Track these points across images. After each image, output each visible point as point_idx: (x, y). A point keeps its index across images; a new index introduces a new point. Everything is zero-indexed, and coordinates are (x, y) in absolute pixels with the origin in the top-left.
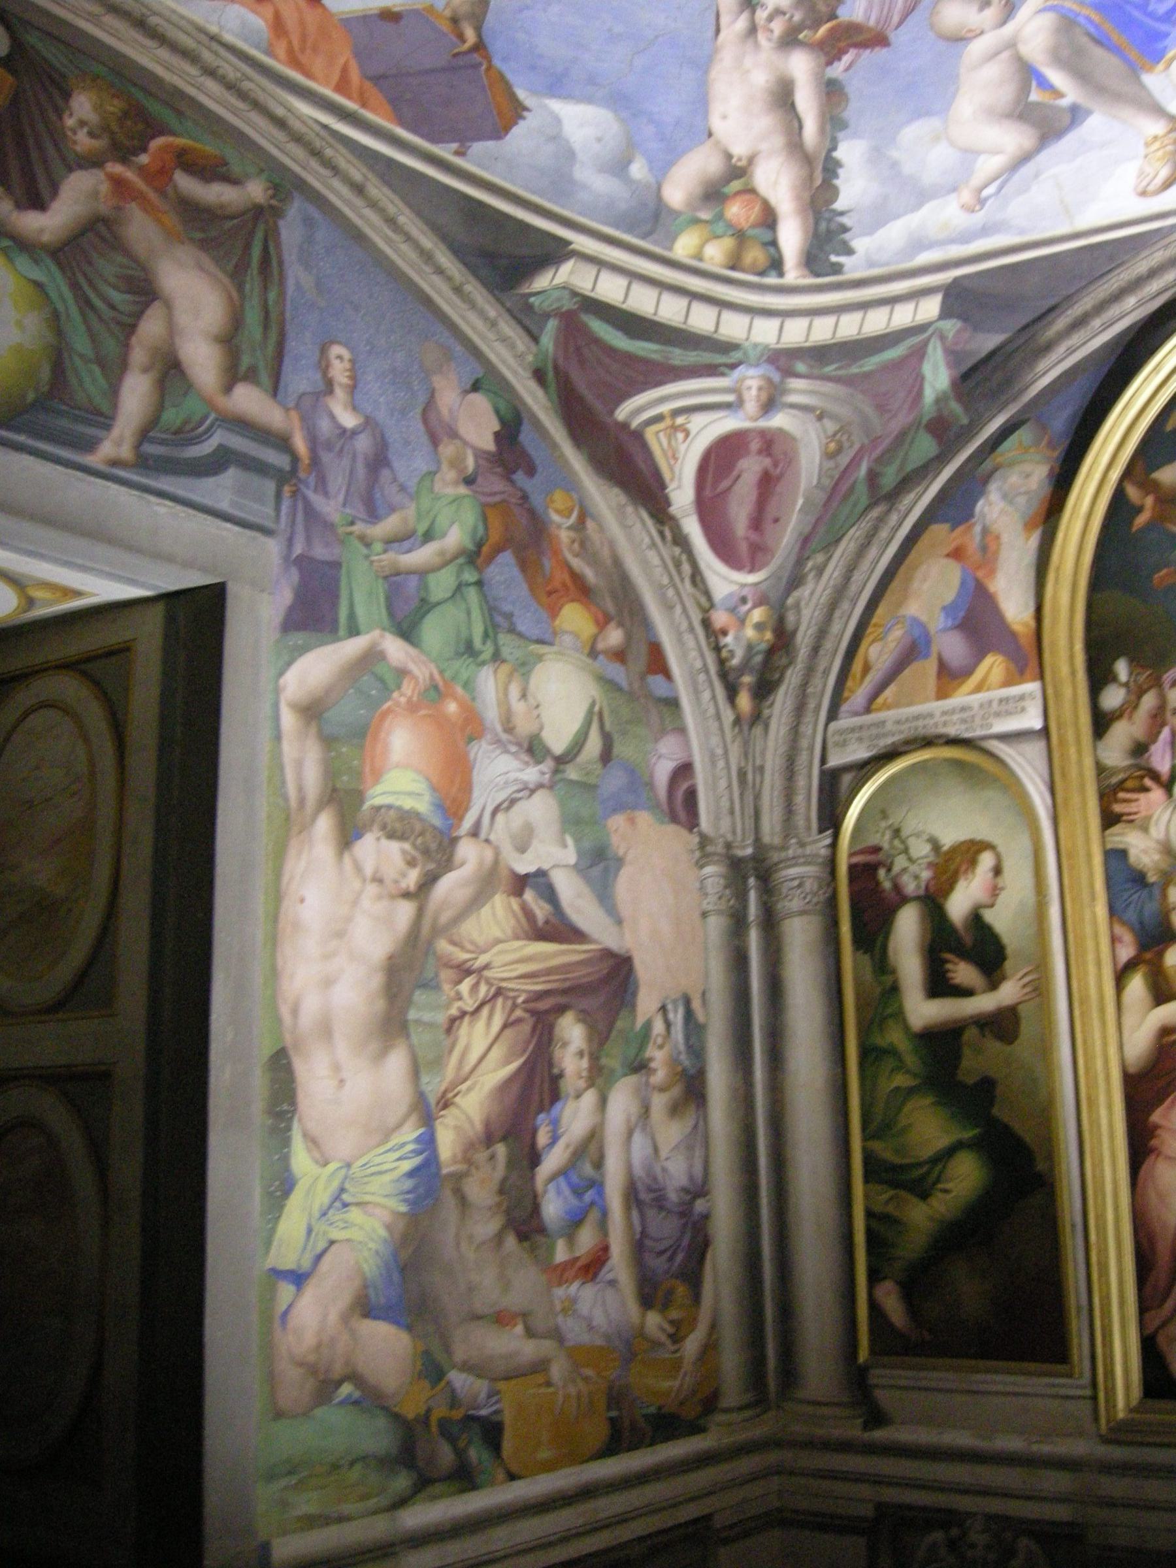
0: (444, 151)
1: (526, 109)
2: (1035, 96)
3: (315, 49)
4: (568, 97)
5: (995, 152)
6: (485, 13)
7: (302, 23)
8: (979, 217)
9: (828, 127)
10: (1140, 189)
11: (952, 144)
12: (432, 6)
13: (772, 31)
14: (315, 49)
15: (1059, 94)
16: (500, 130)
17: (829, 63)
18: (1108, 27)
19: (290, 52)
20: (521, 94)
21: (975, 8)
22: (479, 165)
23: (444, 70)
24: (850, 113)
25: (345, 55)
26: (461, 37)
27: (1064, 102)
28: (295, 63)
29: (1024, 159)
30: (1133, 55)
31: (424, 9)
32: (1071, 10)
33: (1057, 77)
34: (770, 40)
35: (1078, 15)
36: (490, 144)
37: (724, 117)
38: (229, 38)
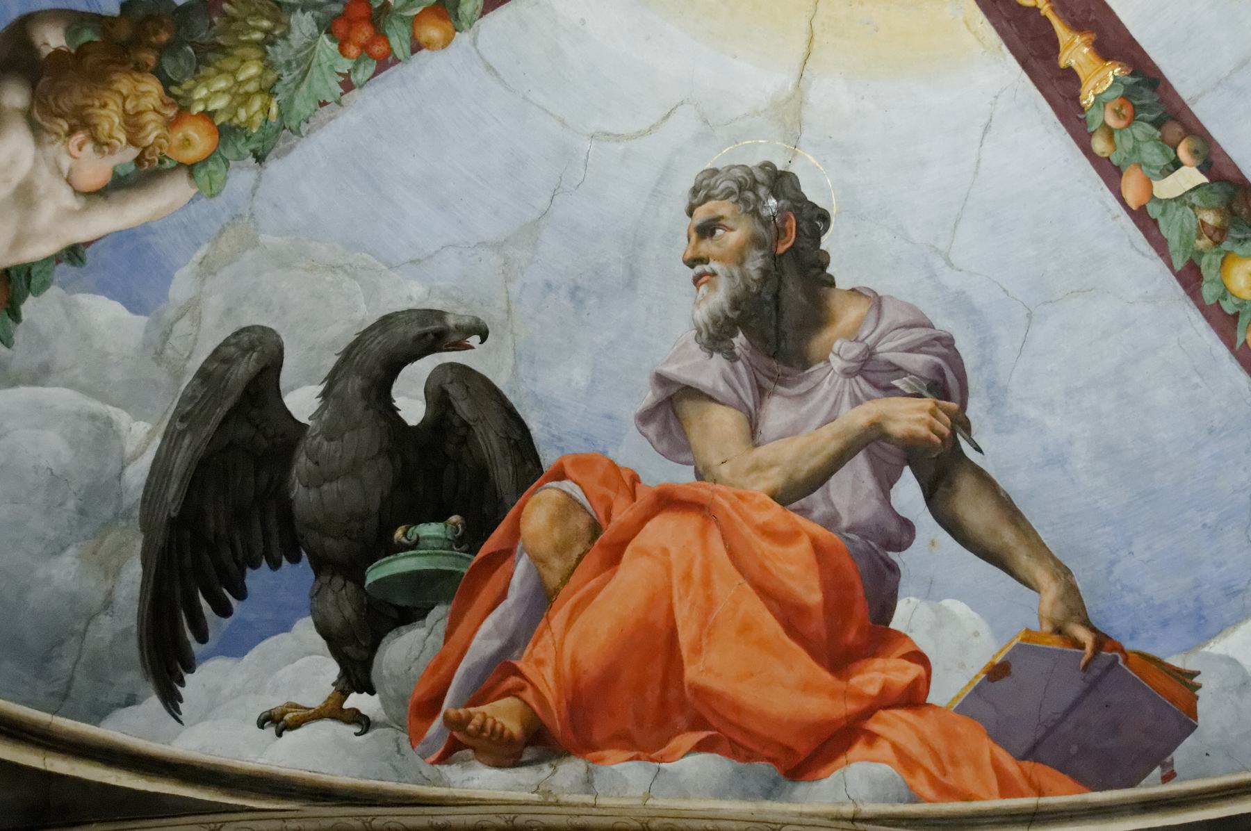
0: (1151, 787)
1: (1194, 674)
3: (954, 762)
4: (1222, 629)
6: (1080, 600)
7: (924, 741)
12: (1028, 631)
14: (954, 762)
16: (1187, 723)
19: (933, 781)
20: (1176, 661)
22: (1196, 777)
23: (1087, 692)
25: (987, 748)
26: (1079, 645)
28: (947, 792)
31: (1023, 640)
36: (1189, 741)
38: (868, 809)
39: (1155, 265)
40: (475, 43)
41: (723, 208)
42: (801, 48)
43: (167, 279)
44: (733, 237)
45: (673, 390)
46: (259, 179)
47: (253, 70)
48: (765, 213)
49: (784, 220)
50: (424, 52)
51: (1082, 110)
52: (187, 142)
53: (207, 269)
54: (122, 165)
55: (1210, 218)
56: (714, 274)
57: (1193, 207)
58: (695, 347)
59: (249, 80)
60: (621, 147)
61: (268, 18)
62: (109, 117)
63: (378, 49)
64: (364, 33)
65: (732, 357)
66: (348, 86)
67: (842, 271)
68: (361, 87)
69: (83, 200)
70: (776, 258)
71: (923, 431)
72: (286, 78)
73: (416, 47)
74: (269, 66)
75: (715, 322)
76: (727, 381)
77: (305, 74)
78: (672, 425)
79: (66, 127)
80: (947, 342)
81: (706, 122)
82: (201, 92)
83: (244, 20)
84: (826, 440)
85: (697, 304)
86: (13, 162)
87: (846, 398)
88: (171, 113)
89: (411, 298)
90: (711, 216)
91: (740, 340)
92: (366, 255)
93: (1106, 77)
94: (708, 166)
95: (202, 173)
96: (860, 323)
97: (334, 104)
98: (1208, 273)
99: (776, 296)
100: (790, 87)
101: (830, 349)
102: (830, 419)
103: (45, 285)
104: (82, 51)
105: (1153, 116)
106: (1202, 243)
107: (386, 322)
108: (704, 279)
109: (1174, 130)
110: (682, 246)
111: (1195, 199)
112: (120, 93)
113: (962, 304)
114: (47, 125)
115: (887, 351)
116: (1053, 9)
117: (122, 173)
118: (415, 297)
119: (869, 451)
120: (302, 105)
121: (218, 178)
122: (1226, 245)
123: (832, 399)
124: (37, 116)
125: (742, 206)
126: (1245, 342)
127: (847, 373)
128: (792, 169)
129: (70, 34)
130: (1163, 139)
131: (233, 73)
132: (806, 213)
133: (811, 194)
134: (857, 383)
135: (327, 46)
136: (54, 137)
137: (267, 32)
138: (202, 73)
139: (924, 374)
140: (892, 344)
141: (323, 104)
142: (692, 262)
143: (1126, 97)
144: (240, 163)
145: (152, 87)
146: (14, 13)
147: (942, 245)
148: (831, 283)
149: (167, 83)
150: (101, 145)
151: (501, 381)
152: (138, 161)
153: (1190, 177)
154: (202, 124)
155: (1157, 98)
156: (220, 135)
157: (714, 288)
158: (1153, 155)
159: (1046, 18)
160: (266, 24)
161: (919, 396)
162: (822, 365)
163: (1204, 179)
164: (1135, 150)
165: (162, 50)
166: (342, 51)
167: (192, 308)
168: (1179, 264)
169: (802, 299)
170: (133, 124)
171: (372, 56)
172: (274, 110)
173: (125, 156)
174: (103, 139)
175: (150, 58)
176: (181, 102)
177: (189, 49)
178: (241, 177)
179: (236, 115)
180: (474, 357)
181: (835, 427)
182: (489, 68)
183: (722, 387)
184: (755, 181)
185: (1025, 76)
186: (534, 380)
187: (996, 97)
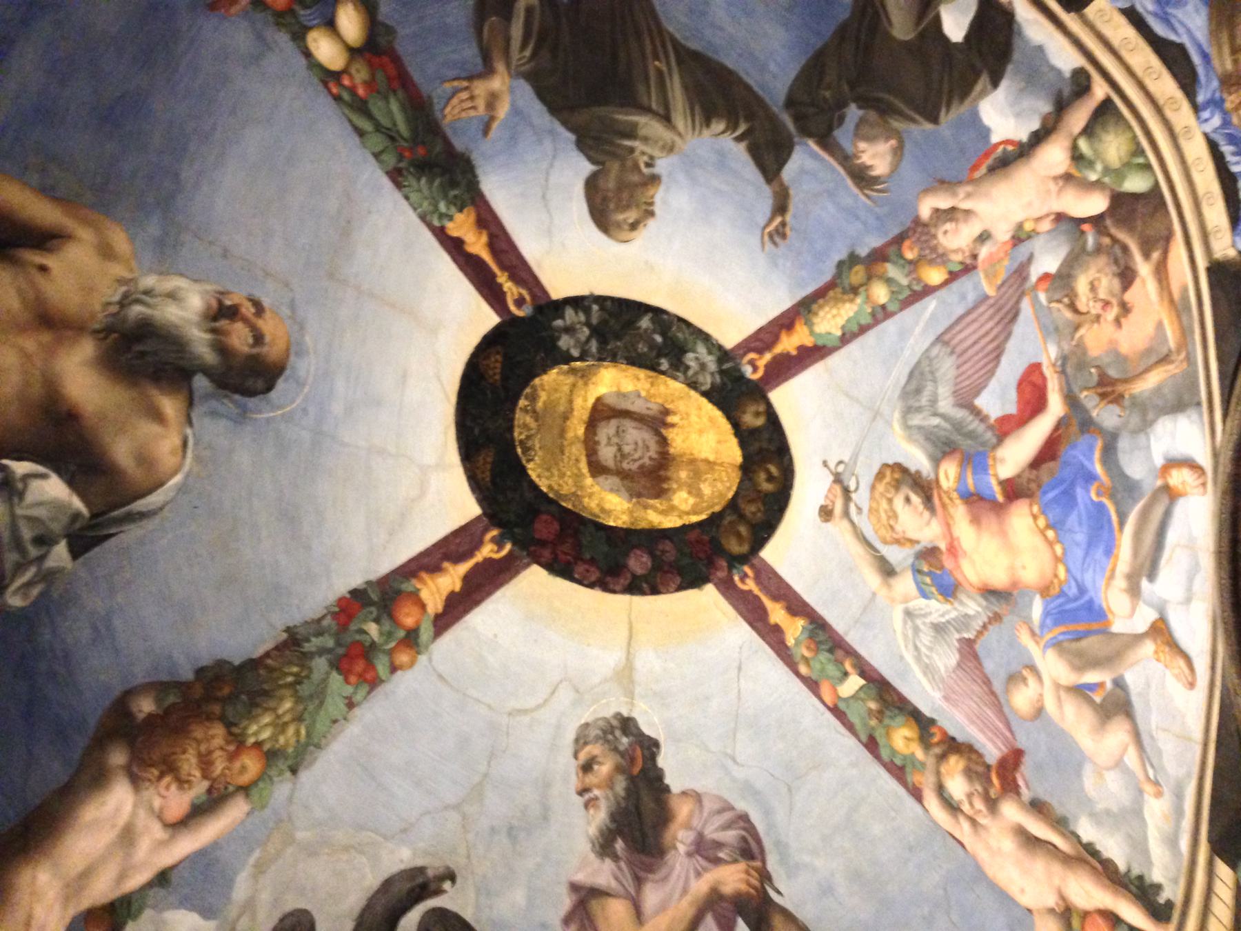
2: (1098, 699)
5: (1125, 750)
8: (1168, 796)
9: (1062, 829)
10: (1188, 686)
11: (1108, 769)
13: (980, 811)
15: (1101, 685)
17: (1018, 793)
18: (1072, 627)
21: (1022, 686)
24: (1059, 810)
27: (1109, 685)
29: (1137, 736)
30: (1095, 626)
32: (1051, 639)
33: (1091, 677)
34: (985, 817)
35: (1055, 638)
37: (1022, 891)
39: (850, 741)
40: (430, 660)
41: (595, 749)
42: (625, 633)
43: (229, 883)
44: (604, 768)
45: (583, 893)
46: (293, 791)
47: (287, 705)
48: (621, 748)
49: (634, 750)
50: (399, 673)
51: (787, 648)
52: (244, 769)
53: (260, 869)
54: (198, 797)
55: (873, 705)
56: (596, 798)
57: (863, 700)
58: (592, 856)
59: (285, 713)
60: (526, 719)
61: (297, 665)
62: (188, 760)
63: (368, 676)
64: (359, 666)
65: (616, 858)
66: (351, 705)
67: (675, 781)
68: (359, 704)
69: (170, 830)
70: (632, 779)
71: (743, 887)
72: (311, 707)
73: (394, 669)
74: (299, 699)
75: (602, 833)
76: (616, 878)
77: (322, 703)
78: (586, 922)
79: (156, 772)
80: (744, 818)
81: (577, 691)
82: (254, 728)
83: (280, 669)
84: (684, 908)
85: (589, 823)
86: (118, 810)
87: (692, 875)
88: (232, 748)
89: (402, 861)
90: (589, 756)
91: (619, 845)
92: (370, 833)
93: (796, 628)
94: (583, 721)
95: (254, 792)
96: (691, 815)
97: (343, 721)
98: (881, 741)
99: (637, 807)
100: (624, 660)
101: (675, 838)
102: (685, 891)
103: (140, 910)
104: (167, 712)
105: (826, 647)
106: (873, 722)
107: (388, 884)
108: (591, 804)
109: (840, 653)
110: (574, 781)
111: (862, 695)
112: (195, 739)
113: (748, 789)
114: (144, 775)
115: (711, 833)
116: (760, 590)
117: (197, 802)
118: (405, 859)
119: (714, 911)
120: (320, 727)
121: (265, 793)
122: (887, 721)
123: (683, 875)
124: (135, 769)
125: (606, 746)
126: (914, 784)
127: (689, 855)
128: (635, 715)
129: (158, 701)
130: (836, 660)
131: (274, 710)
132: (646, 744)
133: (647, 730)
134: (697, 860)
135: (336, 679)
136: (147, 784)
137: (295, 675)
138: (254, 713)
139: (736, 845)
140: (713, 827)
141: (335, 721)
142: (582, 792)
143: (811, 638)
144: (281, 778)
145: (218, 731)
146: (117, 692)
147: (729, 751)
148: (667, 789)
149: (229, 725)
150: (183, 783)
151: (468, 915)
152: (209, 791)
153: (855, 682)
154: (254, 753)
155: (827, 636)
156: (268, 759)
157: (597, 807)
158: (832, 670)
159: (757, 597)
160: (295, 669)
161: (735, 861)
162: (673, 852)
163: (862, 682)
164: (823, 670)
165: (225, 701)
166: (347, 681)
167: (249, 905)
168: (864, 738)
169: (652, 805)
170: (205, 763)
171: (365, 681)
172: (303, 732)
173: (199, 788)
174: (184, 777)
175: (217, 709)
176: (240, 738)
177: (244, 697)
178: (281, 790)
179: (277, 741)
180: (450, 900)
181: (688, 898)
182: (440, 677)
183: (614, 884)
184: (612, 727)
185: (754, 634)
186: (491, 908)
187: (741, 648)
